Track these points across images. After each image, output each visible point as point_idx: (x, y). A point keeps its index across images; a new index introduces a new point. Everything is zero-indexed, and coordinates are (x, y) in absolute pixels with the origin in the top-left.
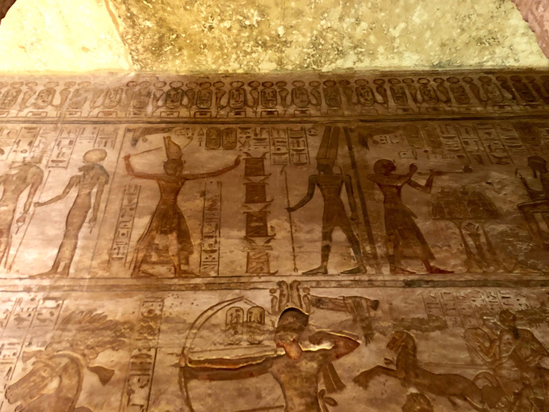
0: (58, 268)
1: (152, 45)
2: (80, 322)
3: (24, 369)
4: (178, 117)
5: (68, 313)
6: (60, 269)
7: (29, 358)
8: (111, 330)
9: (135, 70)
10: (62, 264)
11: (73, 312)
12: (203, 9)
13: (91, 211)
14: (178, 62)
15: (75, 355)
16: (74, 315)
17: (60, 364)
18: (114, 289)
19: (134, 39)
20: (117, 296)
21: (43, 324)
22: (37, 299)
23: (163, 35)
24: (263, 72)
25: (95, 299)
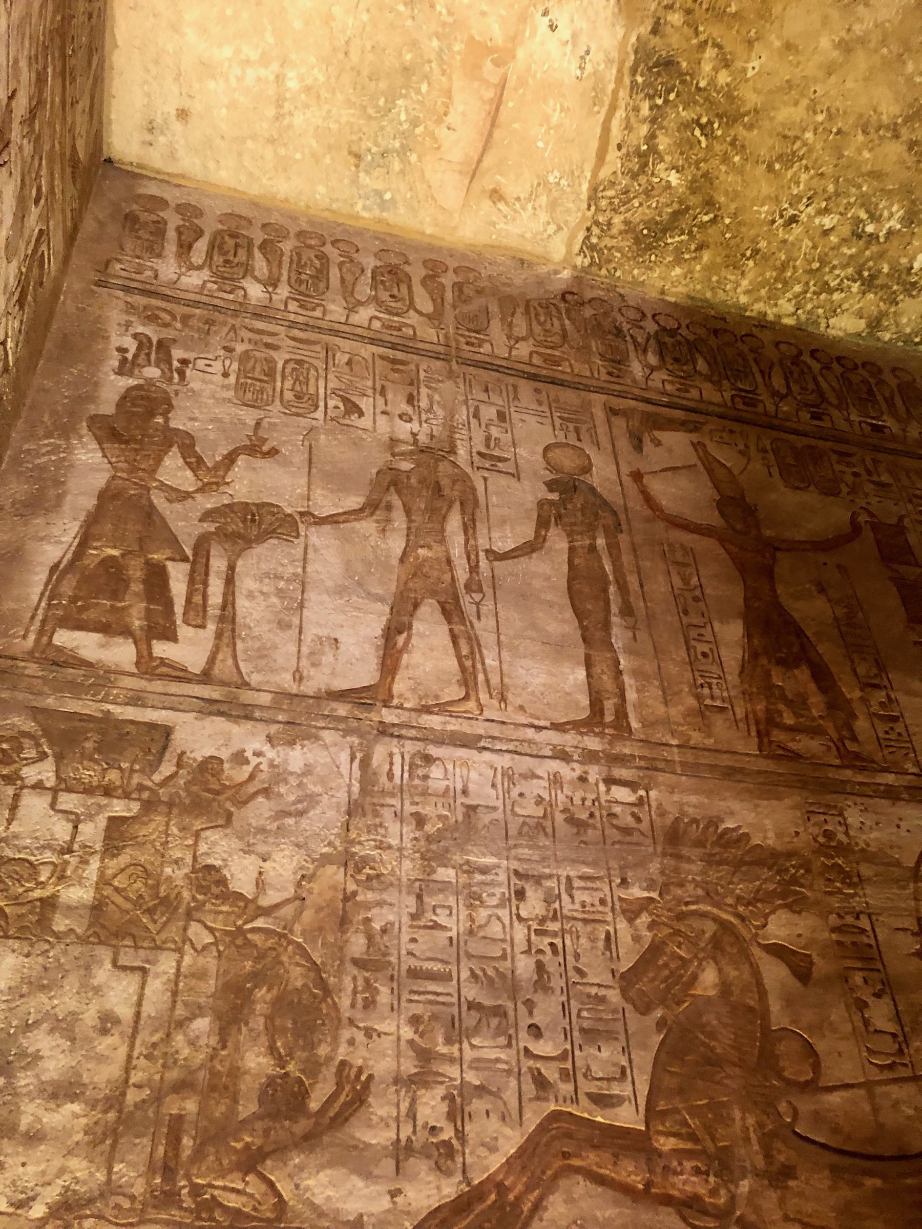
1: (648, 224)
3: (637, 939)
4: (701, 400)
6: (609, 718)
7: (637, 915)
8: (770, 869)
9: (575, 267)
10: (609, 705)
12: (804, 177)
13: (612, 589)
14: (678, 271)
15: (725, 916)
17: (703, 932)
18: (739, 777)
19: (616, 201)
20: (750, 791)
21: (628, 839)
22: (592, 779)
23: (688, 208)
24: (832, 332)
25: (709, 793)
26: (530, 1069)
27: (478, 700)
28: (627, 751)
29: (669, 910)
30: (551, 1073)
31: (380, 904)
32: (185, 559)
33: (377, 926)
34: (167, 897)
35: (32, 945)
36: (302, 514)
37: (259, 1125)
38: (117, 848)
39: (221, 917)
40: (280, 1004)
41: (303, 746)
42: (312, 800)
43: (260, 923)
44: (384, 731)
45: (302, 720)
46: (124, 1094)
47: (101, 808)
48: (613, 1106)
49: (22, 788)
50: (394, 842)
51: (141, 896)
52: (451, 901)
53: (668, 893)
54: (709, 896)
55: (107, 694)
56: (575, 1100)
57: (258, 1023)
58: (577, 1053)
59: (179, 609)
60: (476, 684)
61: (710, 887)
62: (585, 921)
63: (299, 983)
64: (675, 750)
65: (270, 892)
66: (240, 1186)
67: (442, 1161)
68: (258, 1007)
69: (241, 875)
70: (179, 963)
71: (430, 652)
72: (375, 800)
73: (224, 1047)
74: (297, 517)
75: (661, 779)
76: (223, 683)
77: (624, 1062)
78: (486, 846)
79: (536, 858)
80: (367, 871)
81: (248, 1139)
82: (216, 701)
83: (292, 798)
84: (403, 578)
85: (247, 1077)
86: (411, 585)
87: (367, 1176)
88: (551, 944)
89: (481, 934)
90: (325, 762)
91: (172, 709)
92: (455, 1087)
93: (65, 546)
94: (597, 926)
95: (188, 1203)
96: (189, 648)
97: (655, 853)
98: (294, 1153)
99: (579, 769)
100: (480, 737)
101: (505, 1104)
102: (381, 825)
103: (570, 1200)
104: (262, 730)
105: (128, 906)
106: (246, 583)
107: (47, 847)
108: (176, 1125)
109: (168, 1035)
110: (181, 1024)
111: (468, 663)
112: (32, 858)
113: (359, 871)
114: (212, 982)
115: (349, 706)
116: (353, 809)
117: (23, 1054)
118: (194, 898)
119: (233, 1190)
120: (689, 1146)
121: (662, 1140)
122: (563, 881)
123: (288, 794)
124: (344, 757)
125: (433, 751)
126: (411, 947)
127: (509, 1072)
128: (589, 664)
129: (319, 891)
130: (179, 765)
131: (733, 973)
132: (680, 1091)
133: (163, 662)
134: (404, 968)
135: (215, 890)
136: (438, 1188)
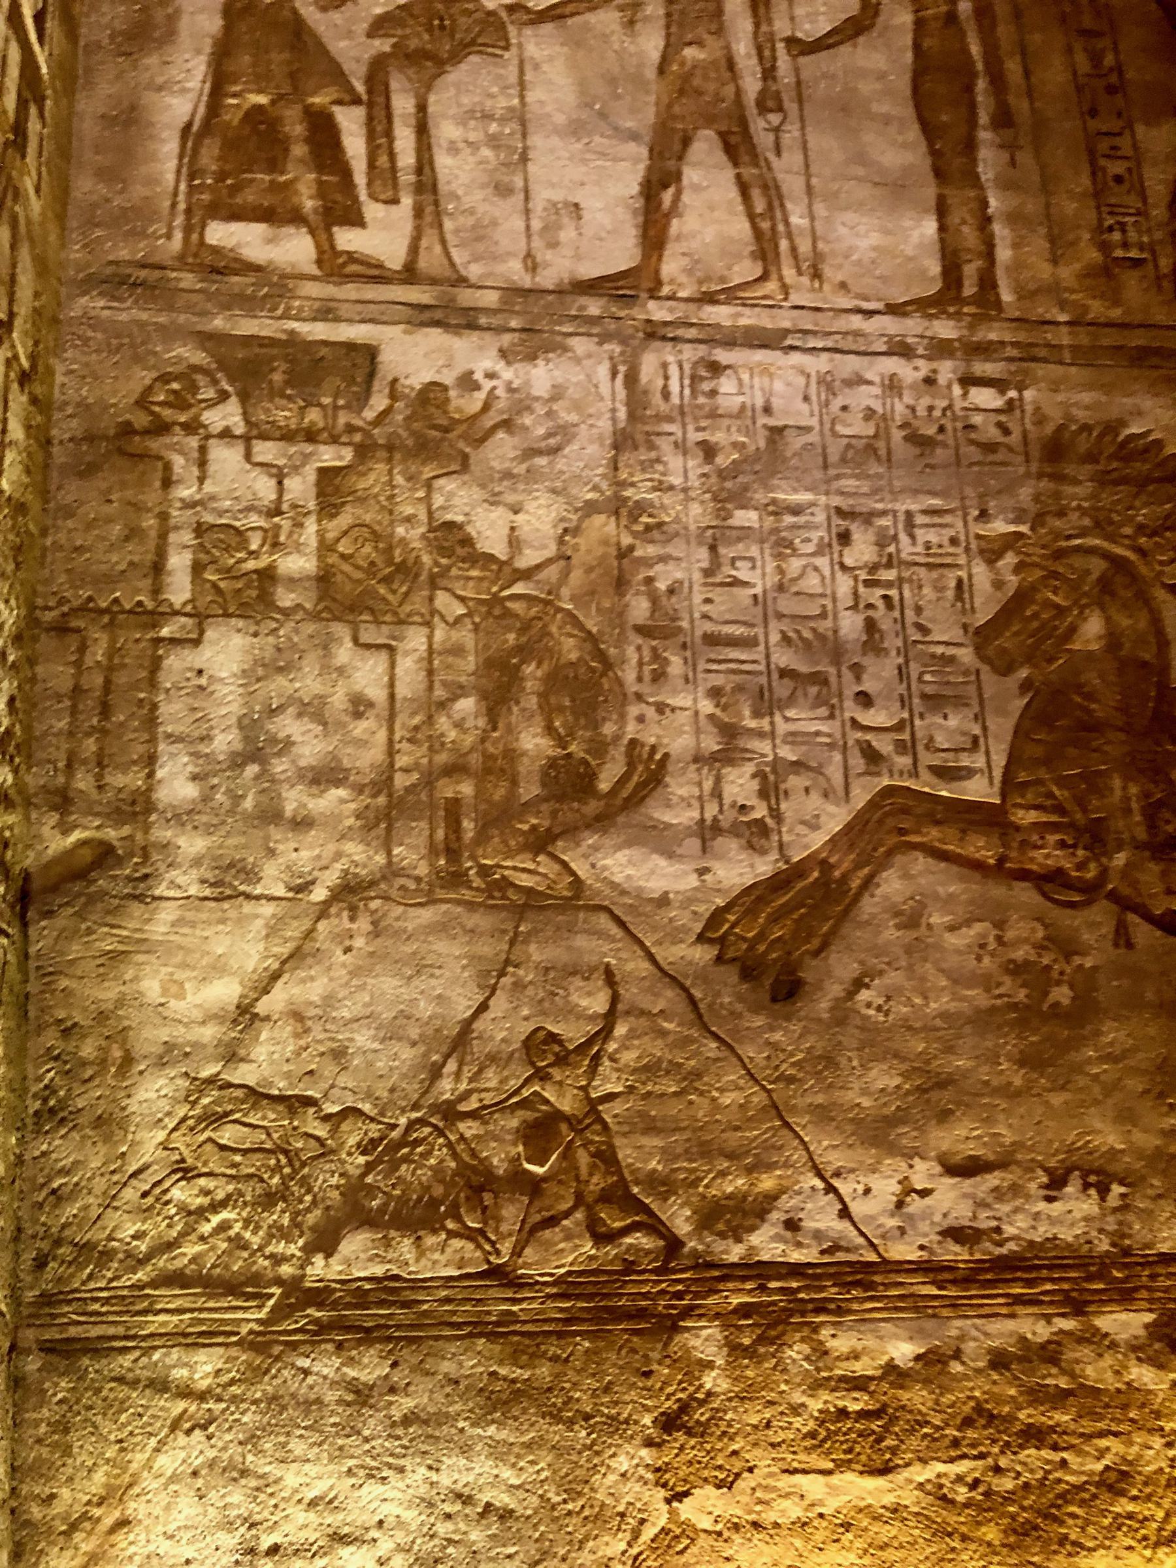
0: (961, 285)
2: (1091, 458)
3: (998, 584)
5: (1049, 429)
6: (969, 290)
7: (1000, 555)
10: (970, 271)
11: (1061, 428)
13: (981, 84)
15: (1119, 551)
16: (1067, 435)
17: (1088, 572)
18: (1155, 361)
21: (991, 458)
22: (942, 380)
25: (1107, 388)
26: (858, 741)
27: (781, 278)
28: (993, 336)
29: (1043, 547)
30: (883, 744)
31: (663, 559)
32: (356, 101)
33: (662, 586)
34: (404, 562)
35: (258, 623)
36: (511, 9)
37: (544, 807)
38: (335, 506)
39: (471, 584)
40: (556, 680)
41: (548, 361)
42: (565, 433)
43: (519, 588)
44: (654, 333)
45: (543, 325)
46: (391, 778)
47: (306, 457)
48: (961, 778)
49: (208, 437)
50: (677, 481)
51: (372, 563)
52: (754, 551)
53: (1043, 525)
54: (1101, 525)
55: (288, 308)
56: (914, 773)
57: (532, 702)
58: (917, 722)
59: (360, 179)
60: (778, 255)
61: (1101, 516)
62: (930, 566)
63: (573, 656)
64: (1065, 330)
65: (527, 551)
66: (532, 866)
67: (755, 840)
68: (529, 684)
69: (489, 531)
70: (430, 637)
71: (710, 214)
72: (647, 428)
73: (495, 729)
74: (504, 14)
75: (1040, 373)
76: (434, 281)
77: (977, 730)
78: (798, 480)
79: (865, 490)
80: (645, 519)
81: (534, 821)
82: (427, 307)
83: (541, 431)
84: (665, 100)
85: (525, 760)
86: (677, 109)
87: (670, 855)
88: (885, 597)
89: (794, 589)
90: (578, 379)
91: (371, 321)
92: (767, 764)
93: (192, 96)
94: (945, 571)
95: (477, 882)
96: (382, 234)
97: (1027, 475)
98: (586, 833)
99: (925, 367)
100: (786, 332)
101: (828, 780)
102: (658, 460)
103: (906, 876)
104: (492, 343)
105: (358, 575)
106: (446, 131)
107: (249, 509)
108: (453, 810)
109: (430, 717)
110: (442, 705)
111: (765, 225)
112: (237, 524)
113: (635, 520)
114: (471, 658)
115: (603, 301)
116: (622, 442)
117: (273, 740)
118: (436, 564)
119: (524, 870)
120: (1054, 818)
121: (1021, 813)
122: (901, 517)
123: (536, 426)
124: (603, 371)
125: (722, 356)
126: (705, 609)
127: (831, 746)
128: (942, 211)
129: (587, 546)
130: (393, 396)
131: (1125, 622)
132: (1046, 762)
133: (351, 258)
134: (699, 633)
135: (460, 551)
136: (752, 866)
